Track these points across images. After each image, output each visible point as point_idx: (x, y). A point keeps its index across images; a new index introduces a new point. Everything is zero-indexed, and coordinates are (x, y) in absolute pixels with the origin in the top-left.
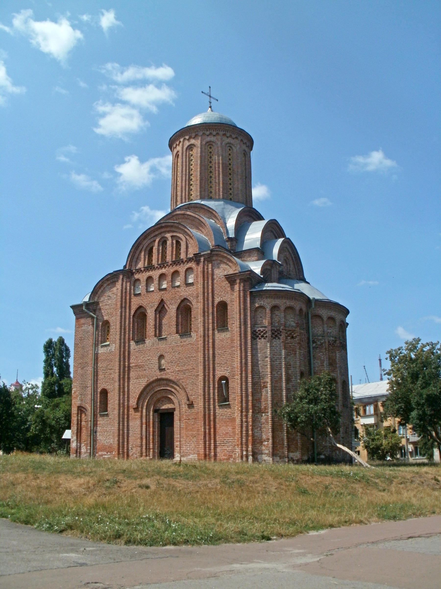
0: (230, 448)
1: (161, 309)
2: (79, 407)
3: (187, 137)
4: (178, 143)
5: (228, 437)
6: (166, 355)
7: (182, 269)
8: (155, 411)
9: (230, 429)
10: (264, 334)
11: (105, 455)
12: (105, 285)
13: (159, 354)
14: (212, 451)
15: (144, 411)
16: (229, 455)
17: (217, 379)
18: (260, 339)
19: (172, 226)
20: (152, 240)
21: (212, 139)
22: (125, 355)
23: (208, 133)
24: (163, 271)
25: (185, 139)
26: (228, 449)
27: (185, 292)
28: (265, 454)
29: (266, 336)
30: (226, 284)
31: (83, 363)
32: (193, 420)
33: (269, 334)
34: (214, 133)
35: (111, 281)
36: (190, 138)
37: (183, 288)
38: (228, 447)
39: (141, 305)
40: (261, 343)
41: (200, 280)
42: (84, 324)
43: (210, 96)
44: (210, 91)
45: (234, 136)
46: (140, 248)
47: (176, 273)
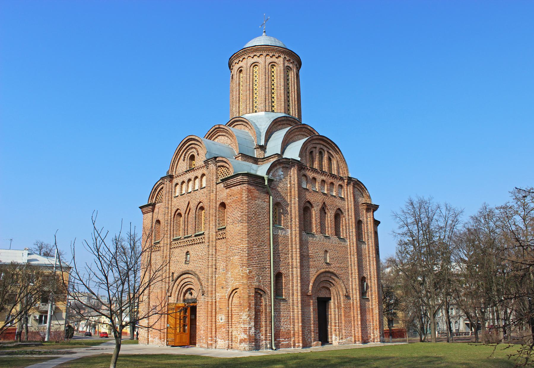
1: (323, 210)
3: (288, 58)
4: (277, 55)
7: (337, 183)
12: (278, 167)
20: (314, 145)
24: (324, 178)
25: (285, 58)
27: (339, 203)
41: (351, 198)
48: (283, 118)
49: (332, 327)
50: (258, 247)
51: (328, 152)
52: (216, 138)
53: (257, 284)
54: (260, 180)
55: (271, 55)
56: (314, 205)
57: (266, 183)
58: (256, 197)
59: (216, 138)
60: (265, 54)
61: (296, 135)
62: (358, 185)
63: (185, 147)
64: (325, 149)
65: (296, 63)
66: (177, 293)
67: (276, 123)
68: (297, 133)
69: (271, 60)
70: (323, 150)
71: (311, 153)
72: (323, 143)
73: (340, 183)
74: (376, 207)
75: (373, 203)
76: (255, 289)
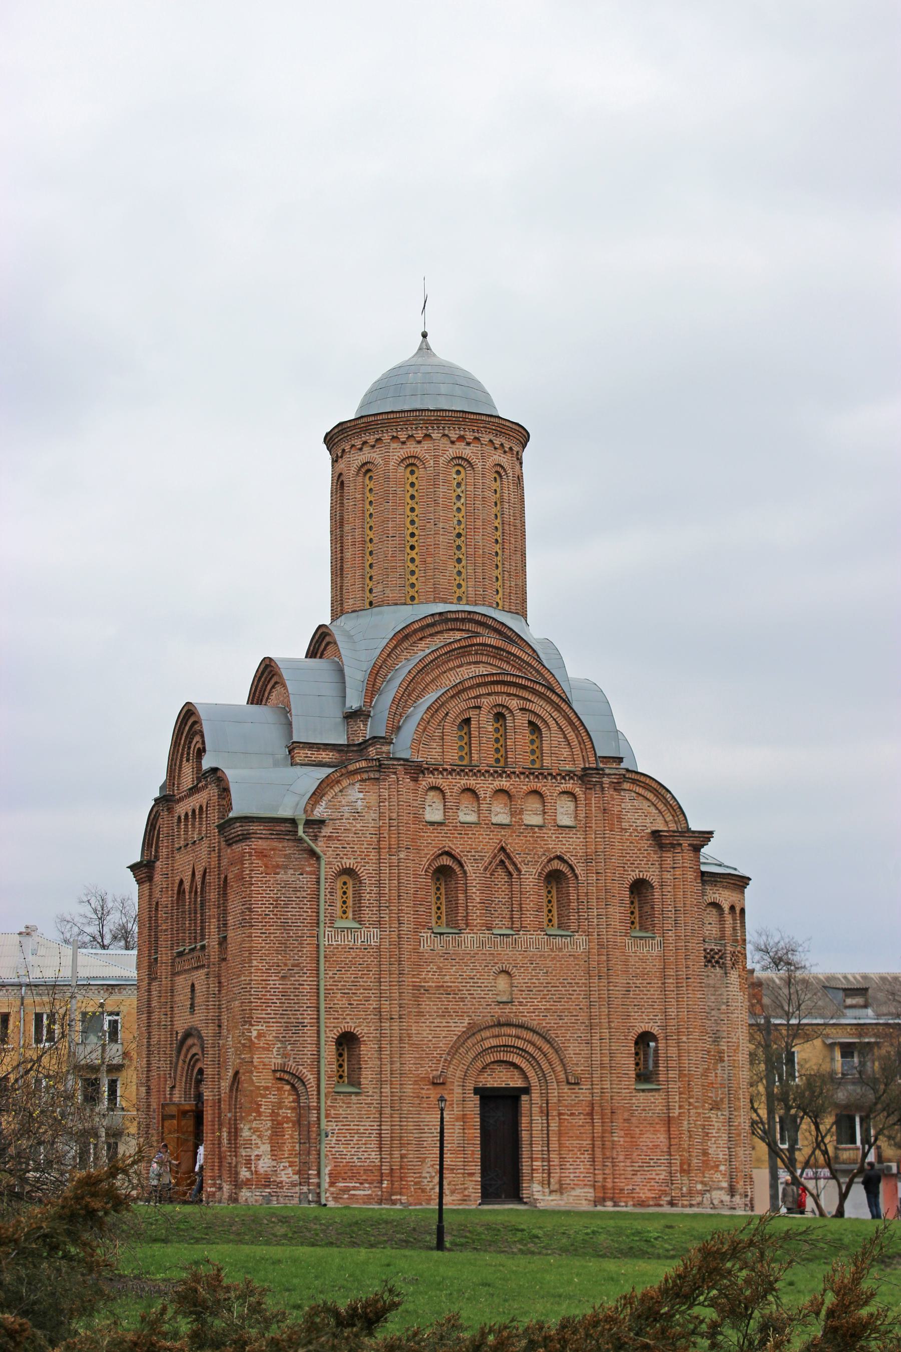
0: (662, 1177)
3: (454, 436)
4: (419, 435)
5: (659, 1154)
8: (477, 1091)
9: (662, 1139)
10: (721, 958)
11: (354, 1188)
12: (345, 783)
15: (458, 1090)
16: (660, 1190)
17: (633, 1036)
18: (713, 966)
19: (525, 688)
20: (472, 703)
24: (504, 783)
26: (657, 1177)
28: (721, 1189)
29: (723, 963)
31: (286, 965)
32: (582, 1117)
35: (365, 776)
36: (461, 438)
37: (550, 834)
38: (657, 1174)
39: (446, 849)
40: (716, 976)
42: (286, 868)
46: (441, 714)
48: (430, 620)
49: (532, 1162)
50: (283, 978)
51: (521, 709)
52: (273, 687)
53: (280, 1061)
54: (288, 827)
55: (403, 436)
56: (464, 859)
57: (301, 832)
58: (278, 866)
59: (273, 687)
60: (386, 437)
61: (451, 669)
62: (634, 782)
63: (187, 728)
64: (514, 703)
65: (485, 438)
66: (184, 1079)
67: (406, 637)
68: (451, 665)
69: (403, 452)
70: (507, 708)
71: (467, 721)
72: (505, 689)
73: (569, 785)
74: (706, 836)
75: (695, 825)
76: (275, 1071)
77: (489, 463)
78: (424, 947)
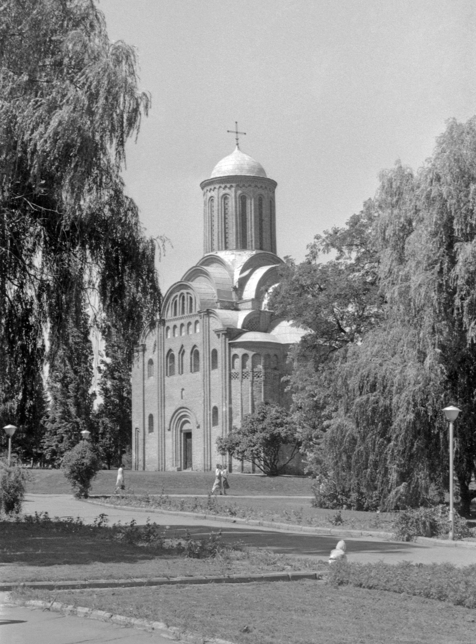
1: (182, 352)
2: (136, 428)
3: (209, 189)
6: (185, 388)
8: (181, 431)
13: (181, 388)
14: (209, 462)
21: (227, 191)
22: (162, 388)
23: (223, 186)
24: (182, 321)
30: (215, 336)
33: (240, 376)
34: (228, 185)
43: (237, 133)
44: (237, 126)
45: (246, 185)
47: (189, 324)
77: (221, 194)
78: (166, 383)
